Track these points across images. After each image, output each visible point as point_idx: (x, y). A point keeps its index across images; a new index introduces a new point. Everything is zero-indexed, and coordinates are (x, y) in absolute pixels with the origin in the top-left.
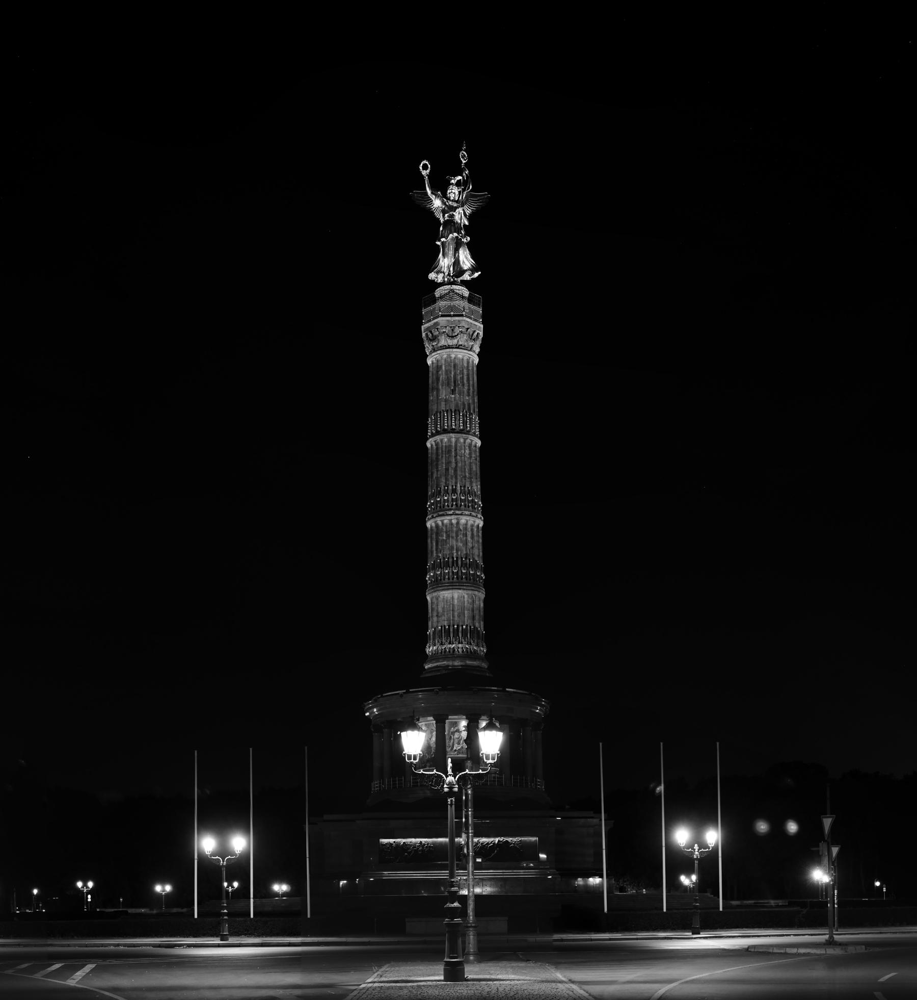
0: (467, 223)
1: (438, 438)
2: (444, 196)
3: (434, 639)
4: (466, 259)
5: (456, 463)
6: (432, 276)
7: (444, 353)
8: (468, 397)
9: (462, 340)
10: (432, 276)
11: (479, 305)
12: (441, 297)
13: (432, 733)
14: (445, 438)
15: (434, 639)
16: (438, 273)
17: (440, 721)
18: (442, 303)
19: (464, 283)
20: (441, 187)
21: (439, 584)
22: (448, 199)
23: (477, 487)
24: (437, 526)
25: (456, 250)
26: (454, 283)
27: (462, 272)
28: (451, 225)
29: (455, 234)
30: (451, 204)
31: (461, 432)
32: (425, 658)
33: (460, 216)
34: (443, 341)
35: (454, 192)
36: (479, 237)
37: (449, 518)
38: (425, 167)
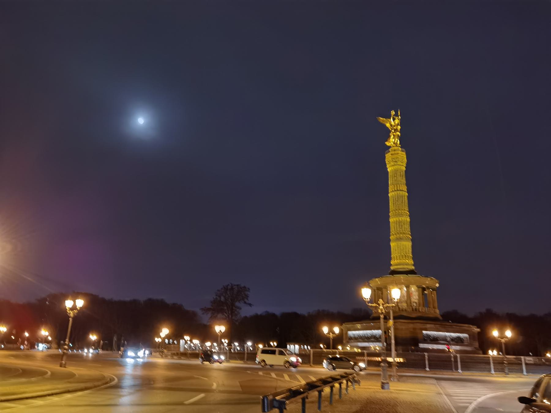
1: (398, 192)
7: (399, 167)
14: (401, 192)
16: (389, 142)
17: (408, 287)
30: (393, 123)
32: (391, 265)
34: (399, 163)
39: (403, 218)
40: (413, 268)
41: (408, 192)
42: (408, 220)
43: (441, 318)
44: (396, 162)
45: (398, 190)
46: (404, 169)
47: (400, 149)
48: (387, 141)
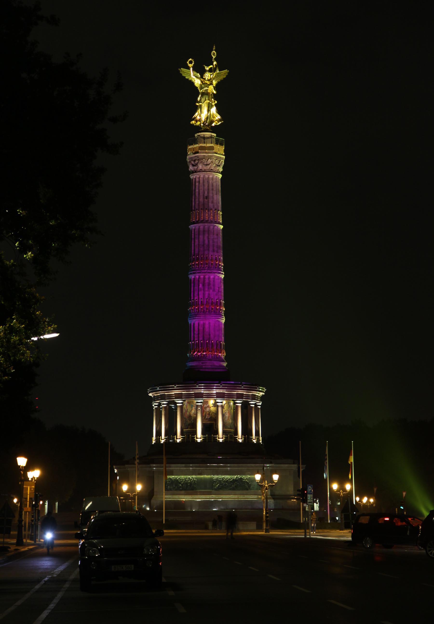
0: (215, 92)
5: (209, 241)
11: (221, 144)
13: (192, 407)
20: (200, 71)
22: (205, 79)
29: (209, 101)
33: (211, 89)
35: (208, 76)
36: (222, 98)
37: (204, 274)
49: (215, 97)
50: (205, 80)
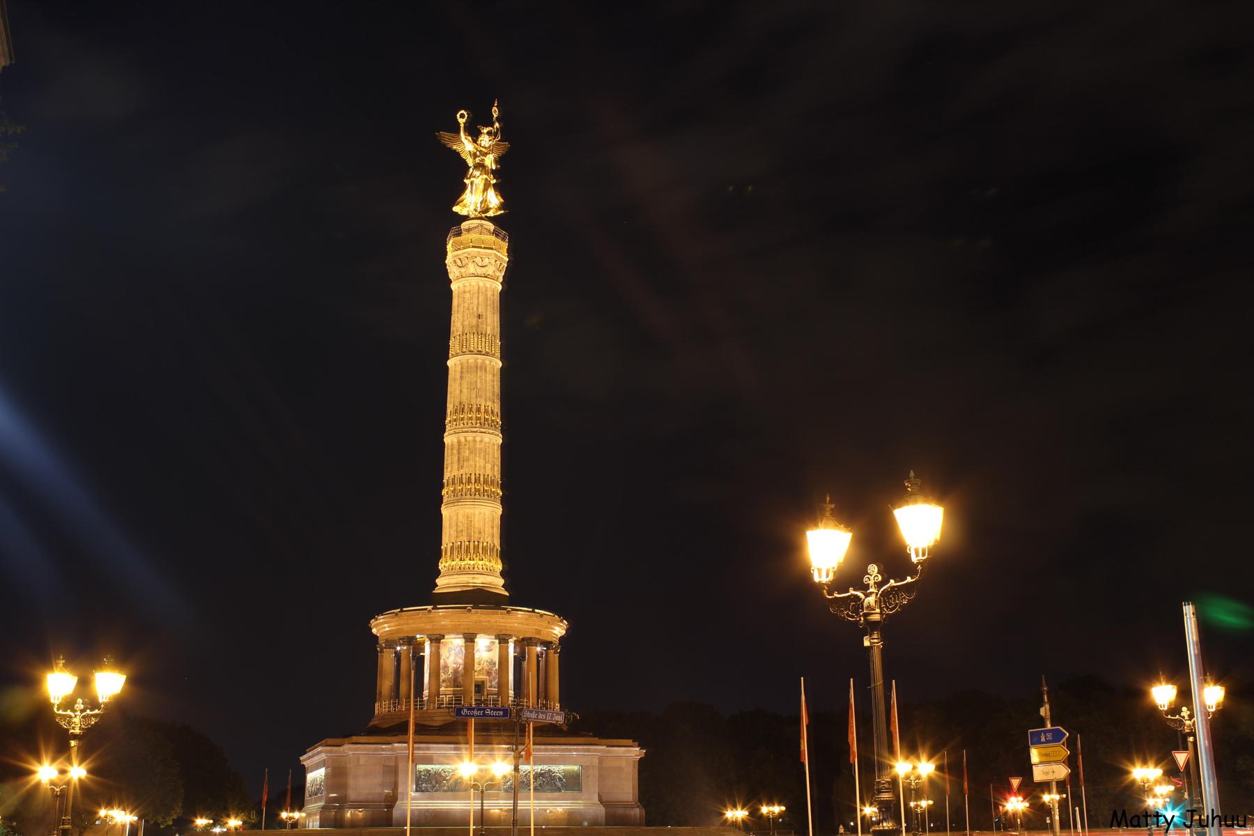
2: (475, 141)
3: (452, 553)
4: (494, 200)
6: (456, 209)
7: (474, 281)
8: (492, 323)
9: (490, 270)
10: (456, 209)
11: (503, 239)
12: (468, 230)
15: (452, 553)
18: (474, 236)
19: (490, 219)
21: (458, 498)
23: (497, 408)
24: (459, 442)
25: (485, 190)
26: (481, 218)
27: (487, 210)
28: (480, 166)
30: (478, 149)
31: (487, 354)
32: (438, 573)
33: (489, 161)
34: (472, 269)
35: (485, 140)
38: (462, 116)
39: (470, 437)
40: (501, 582)
41: (501, 359)
42: (500, 441)
43: (565, 728)
44: (476, 269)
45: (464, 353)
46: (500, 287)
47: (491, 226)
48: (454, 203)
49: (495, 173)
50: (478, 149)
